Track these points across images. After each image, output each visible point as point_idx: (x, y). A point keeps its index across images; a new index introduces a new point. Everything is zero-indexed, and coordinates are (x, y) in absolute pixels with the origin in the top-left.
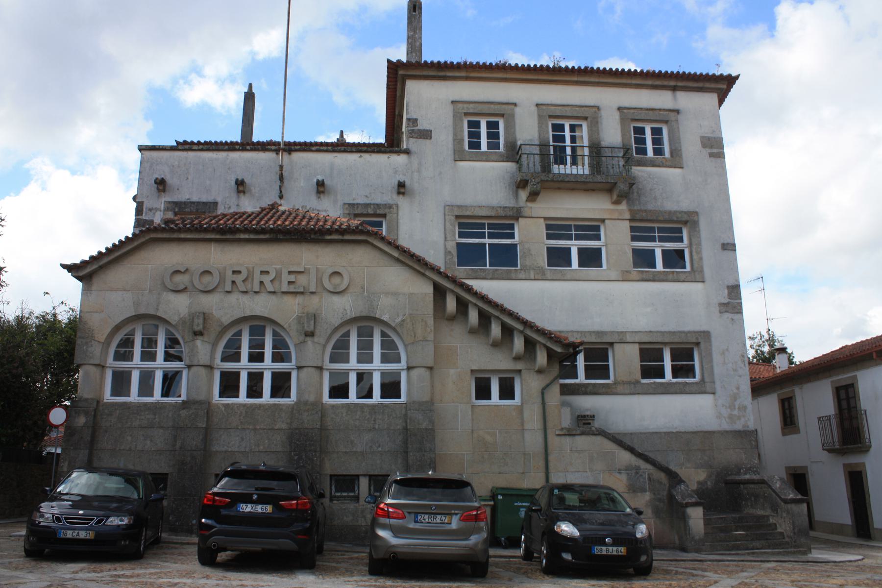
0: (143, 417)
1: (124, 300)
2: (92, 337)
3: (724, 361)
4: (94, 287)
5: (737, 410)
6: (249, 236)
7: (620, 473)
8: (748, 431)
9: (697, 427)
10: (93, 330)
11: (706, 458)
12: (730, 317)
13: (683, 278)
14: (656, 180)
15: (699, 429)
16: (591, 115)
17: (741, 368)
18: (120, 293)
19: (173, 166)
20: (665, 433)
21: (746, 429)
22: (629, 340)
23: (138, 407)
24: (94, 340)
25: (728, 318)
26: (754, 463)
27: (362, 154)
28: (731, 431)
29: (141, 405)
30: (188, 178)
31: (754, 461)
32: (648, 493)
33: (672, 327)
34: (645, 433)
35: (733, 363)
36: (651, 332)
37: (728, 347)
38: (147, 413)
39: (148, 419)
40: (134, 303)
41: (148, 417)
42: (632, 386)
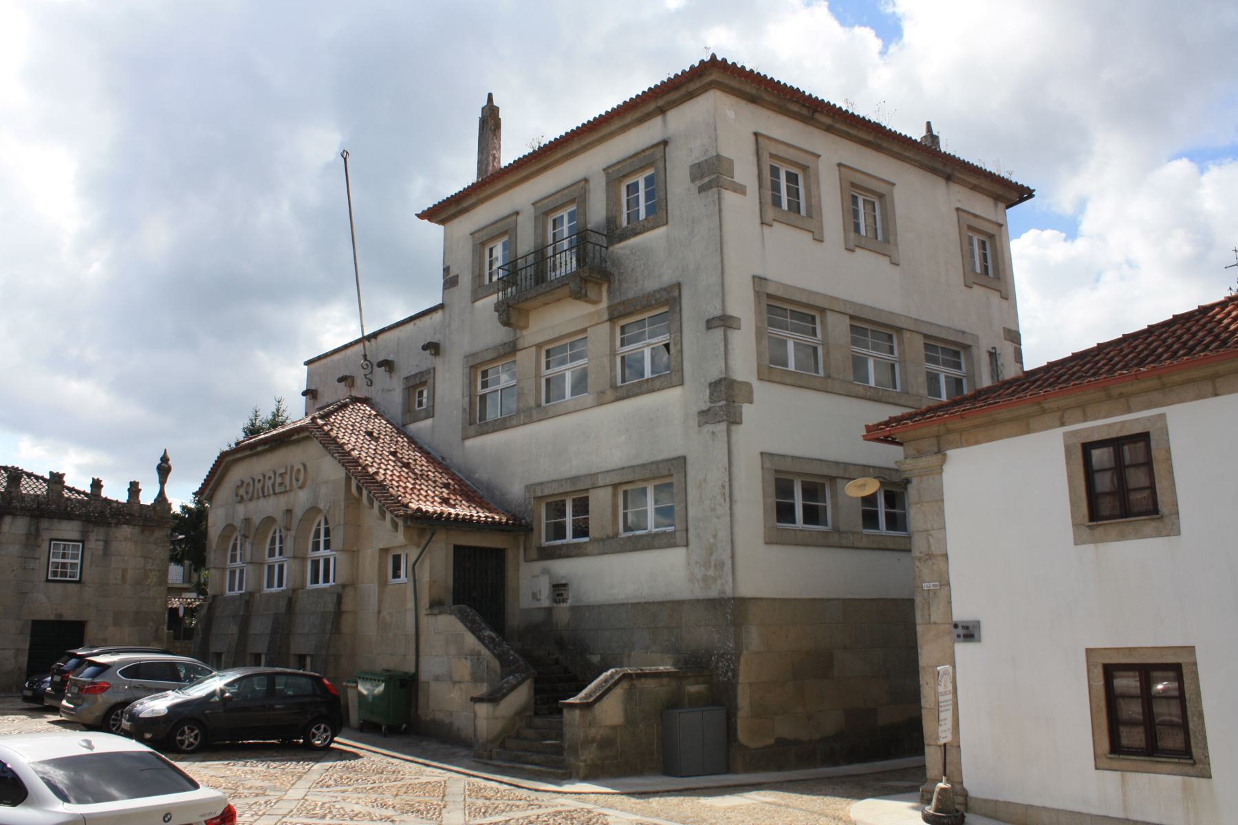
3: (701, 497)
5: (712, 568)
7: (466, 658)
8: (724, 599)
9: (666, 595)
11: (673, 639)
12: (711, 431)
13: (658, 386)
14: (638, 254)
15: (669, 598)
16: (577, 194)
17: (720, 505)
20: (632, 604)
21: (723, 595)
22: (601, 483)
25: (708, 431)
26: (728, 646)
28: (703, 600)
31: (728, 643)
32: (485, 684)
33: (646, 458)
34: (612, 605)
35: (711, 500)
36: (623, 468)
37: (706, 475)
42: (601, 543)
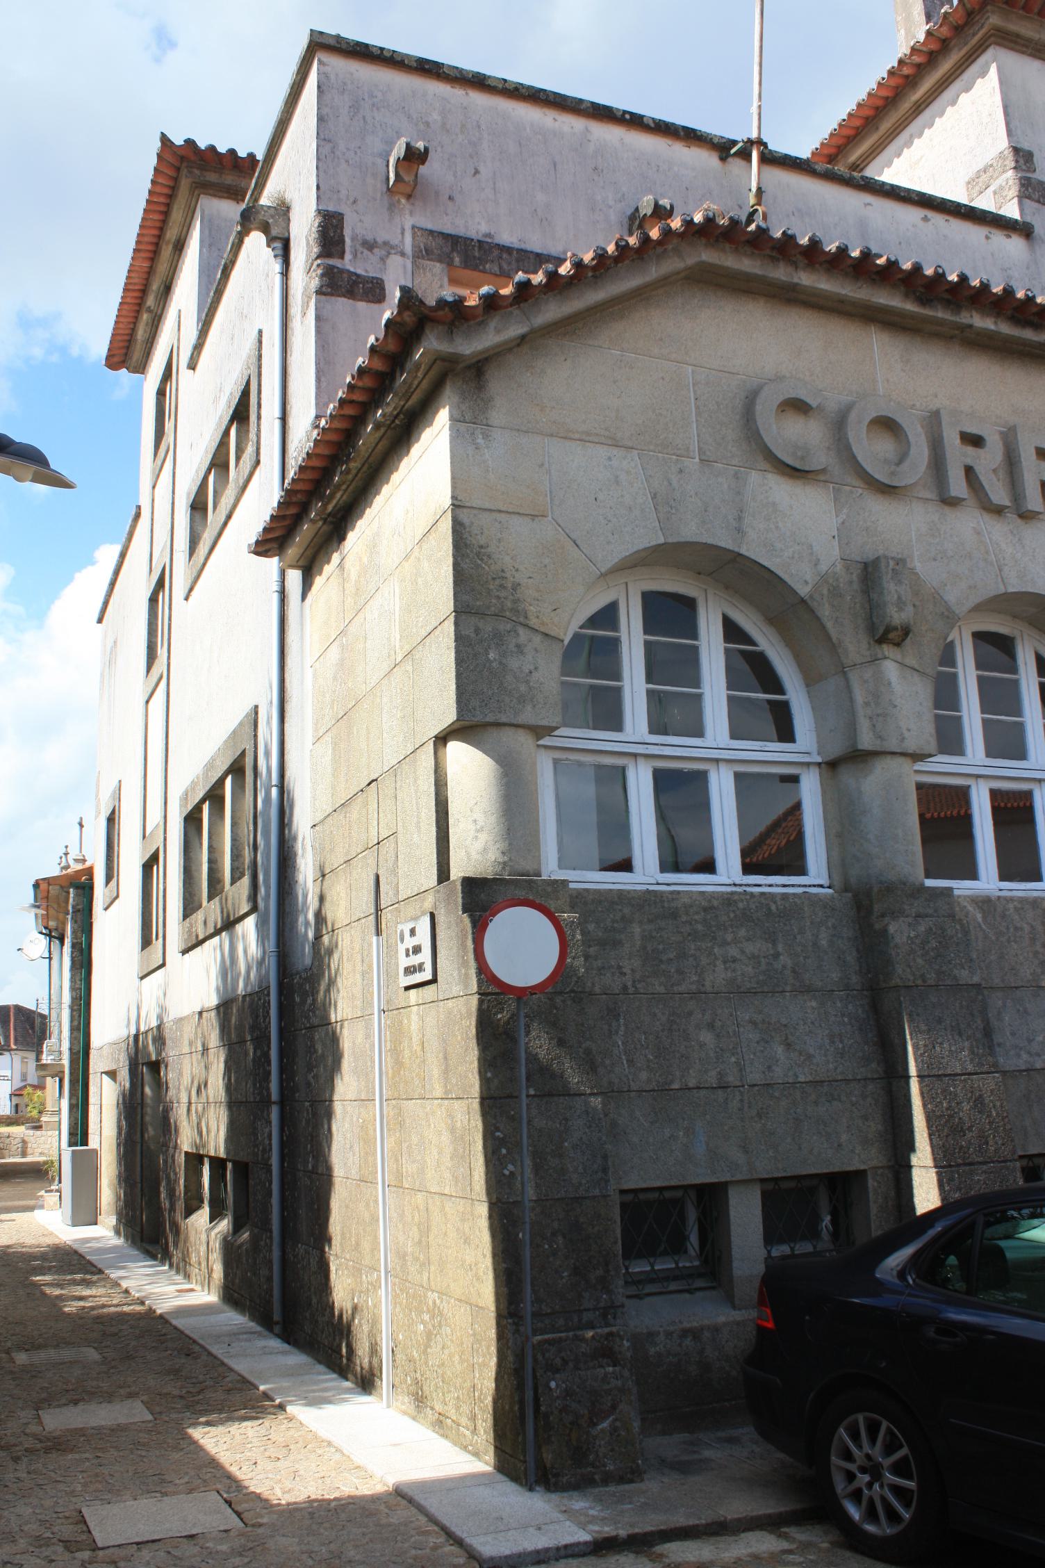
0: (733, 951)
1: (617, 482)
2: (515, 611)
4: (497, 416)
6: (996, 323)
10: (514, 589)
18: (603, 451)
19: (427, 124)
23: (705, 910)
24: (526, 626)
27: (930, 214)
29: (715, 903)
30: (477, 172)
38: (742, 933)
39: (754, 957)
40: (654, 497)
41: (750, 948)
